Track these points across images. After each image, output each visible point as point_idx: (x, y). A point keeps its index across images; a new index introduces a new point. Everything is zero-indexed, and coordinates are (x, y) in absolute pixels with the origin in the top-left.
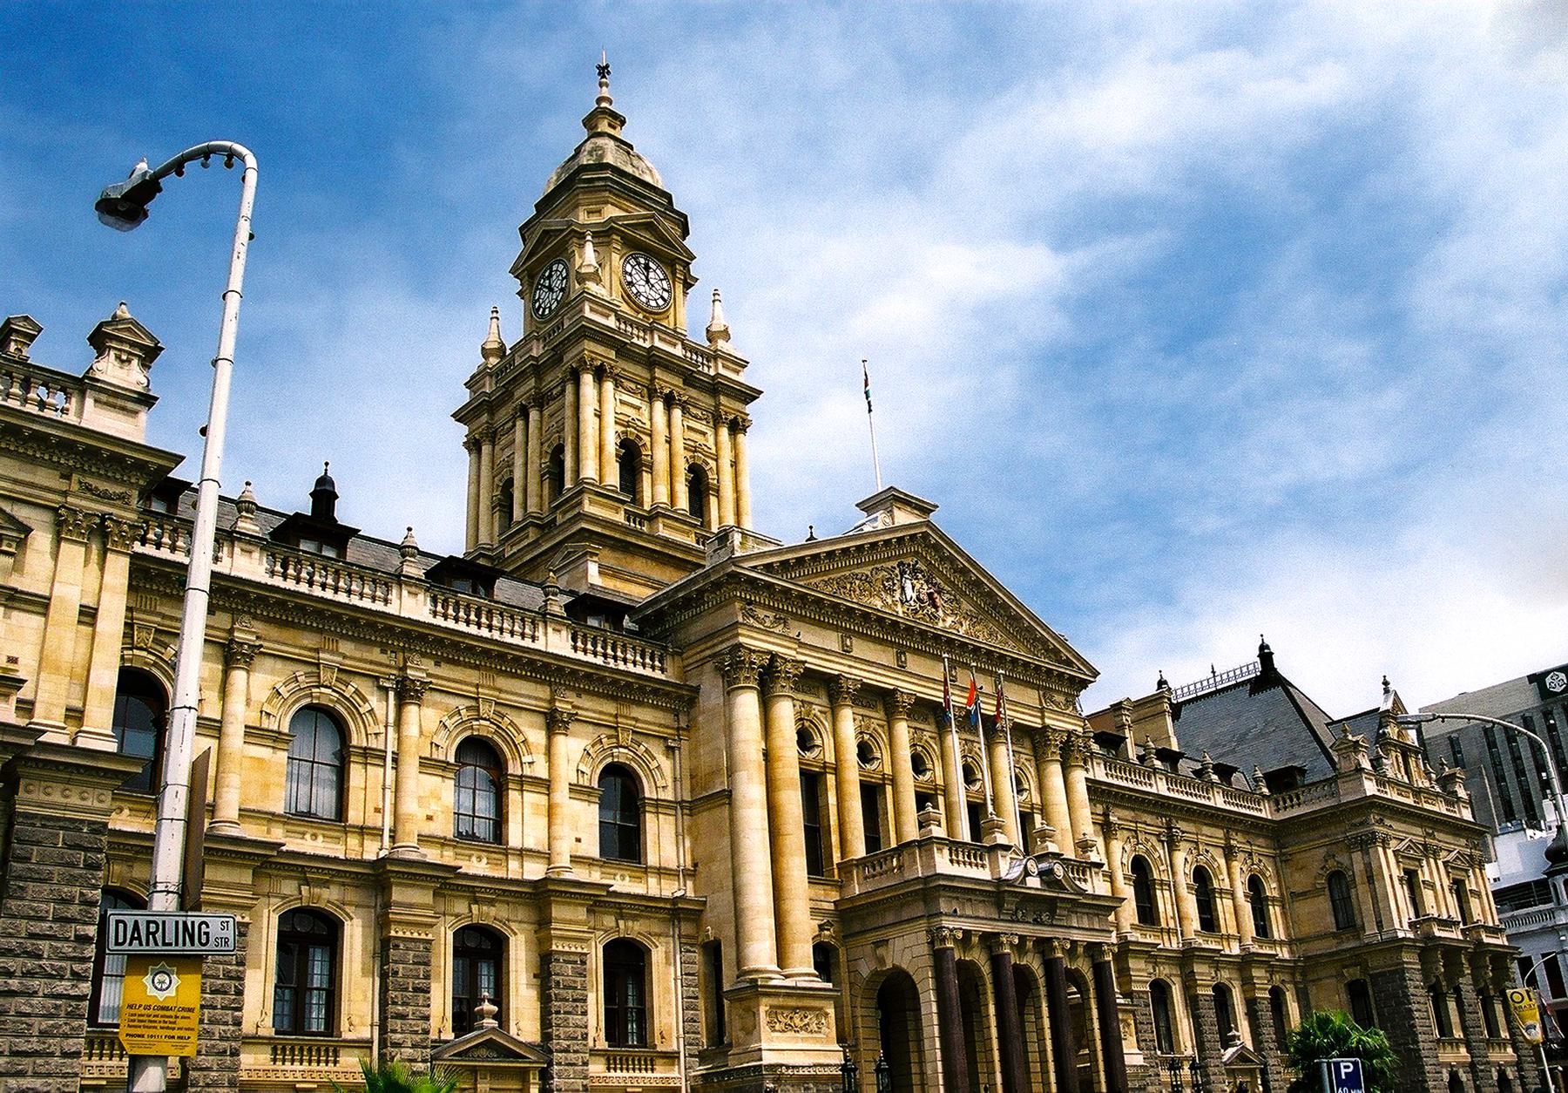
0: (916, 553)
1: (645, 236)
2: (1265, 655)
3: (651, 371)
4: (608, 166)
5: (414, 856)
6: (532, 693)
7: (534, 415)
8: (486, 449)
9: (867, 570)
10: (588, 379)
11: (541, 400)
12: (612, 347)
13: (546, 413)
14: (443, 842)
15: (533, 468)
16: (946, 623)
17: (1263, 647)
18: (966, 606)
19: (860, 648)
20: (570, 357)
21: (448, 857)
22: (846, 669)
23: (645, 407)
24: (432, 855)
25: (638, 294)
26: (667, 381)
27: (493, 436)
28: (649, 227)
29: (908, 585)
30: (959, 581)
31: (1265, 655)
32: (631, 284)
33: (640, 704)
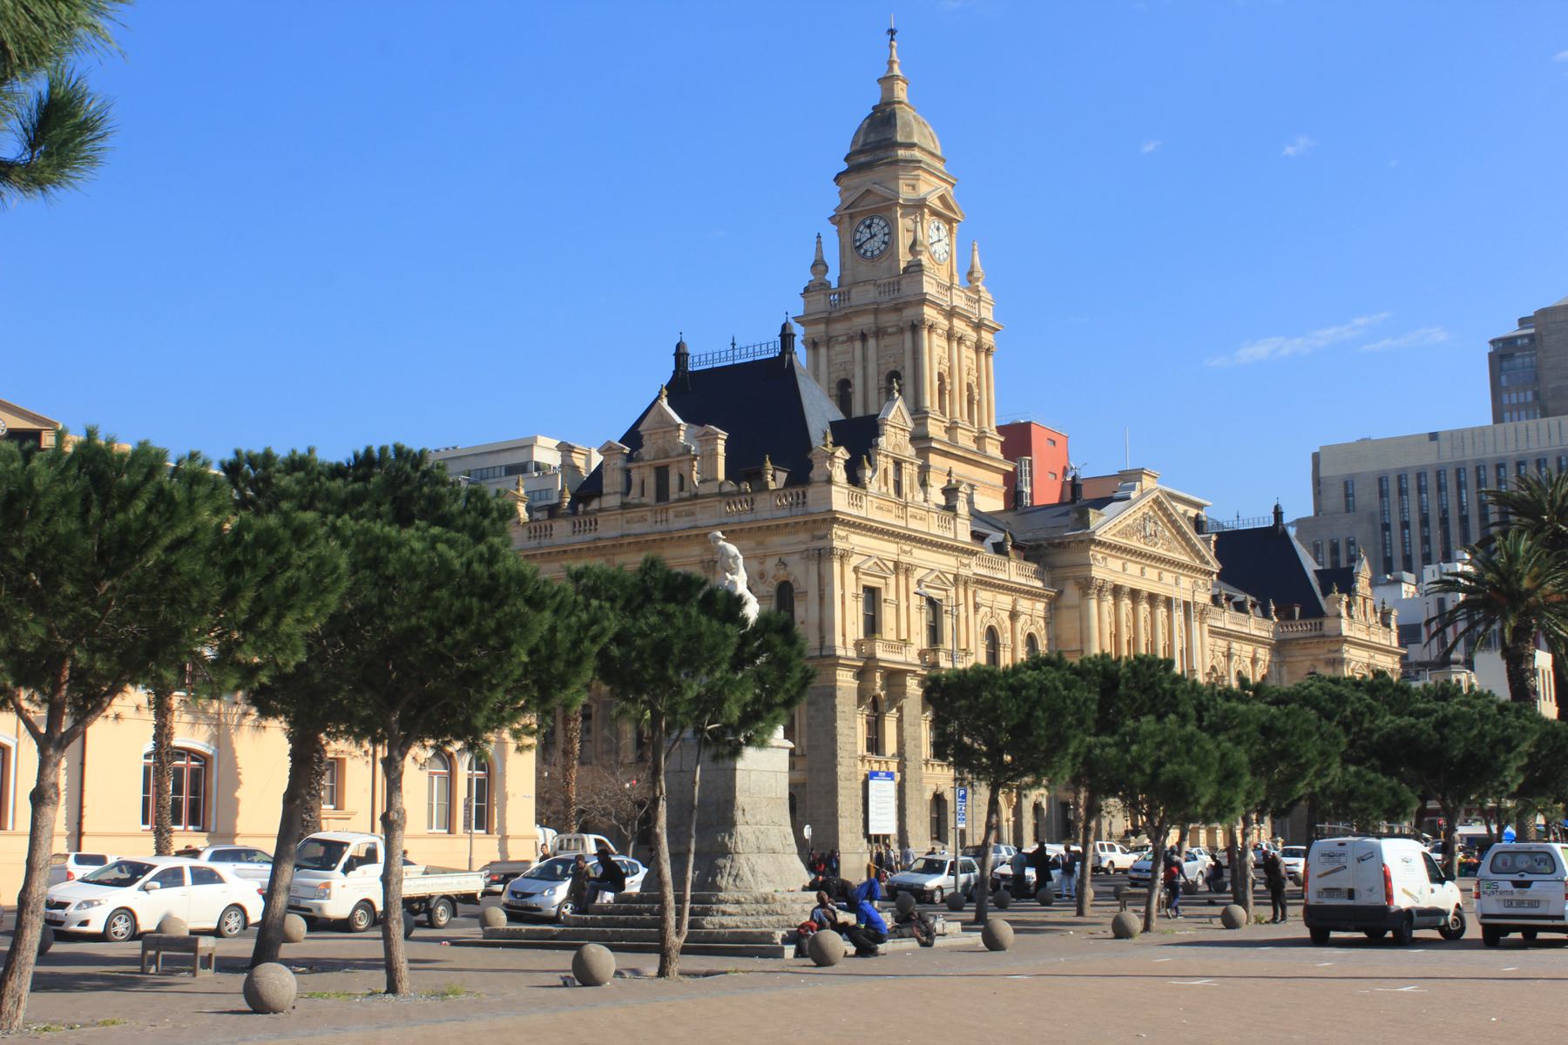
2: (1278, 514)
3: (951, 322)
4: (912, 146)
6: (1005, 600)
7: (872, 342)
8: (823, 351)
10: (925, 333)
11: (879, 333)
13: (883, 343)
15: (872, 383)
17: (1277, 507)
20: (909, 314)
23: (945, 344)
26: (959, 325)
27: (829, 341)
31: (1278, 514)
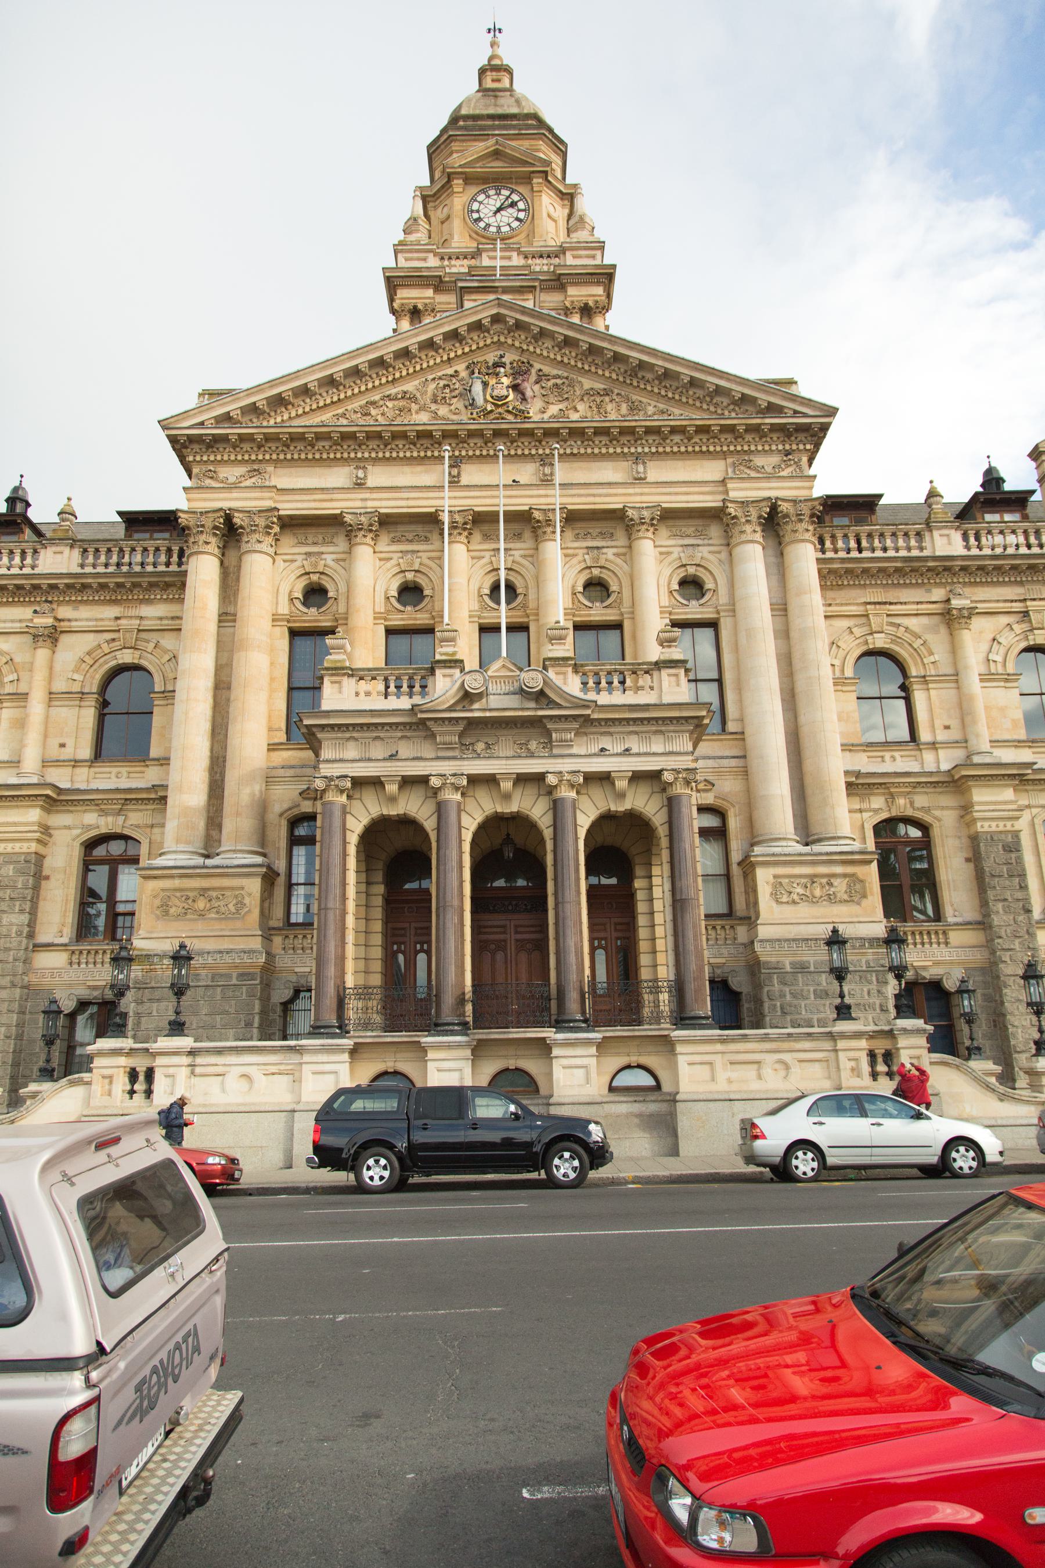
0: (499, 344)
1: (497, 166)
5: (988, 760)
9: (410, 386)
12: (427, 286)
14: (1018, 744)
16: (541, 411)
18: (587, 383)
19: (378, 476)
21: (1025, 755)
22: (359, 504)
24: (1008, 755)
25: (488, 225)
28: (497, 154)
29: (477, 388)
30: (569, 356)
32: (479, 219)
33: (149, 602)
